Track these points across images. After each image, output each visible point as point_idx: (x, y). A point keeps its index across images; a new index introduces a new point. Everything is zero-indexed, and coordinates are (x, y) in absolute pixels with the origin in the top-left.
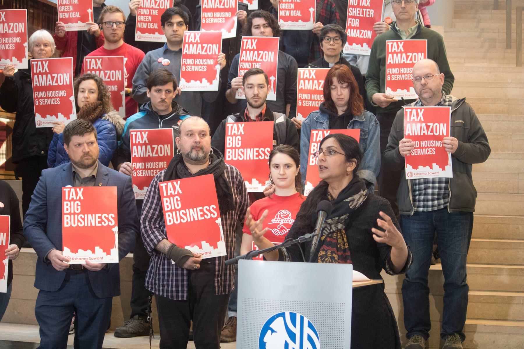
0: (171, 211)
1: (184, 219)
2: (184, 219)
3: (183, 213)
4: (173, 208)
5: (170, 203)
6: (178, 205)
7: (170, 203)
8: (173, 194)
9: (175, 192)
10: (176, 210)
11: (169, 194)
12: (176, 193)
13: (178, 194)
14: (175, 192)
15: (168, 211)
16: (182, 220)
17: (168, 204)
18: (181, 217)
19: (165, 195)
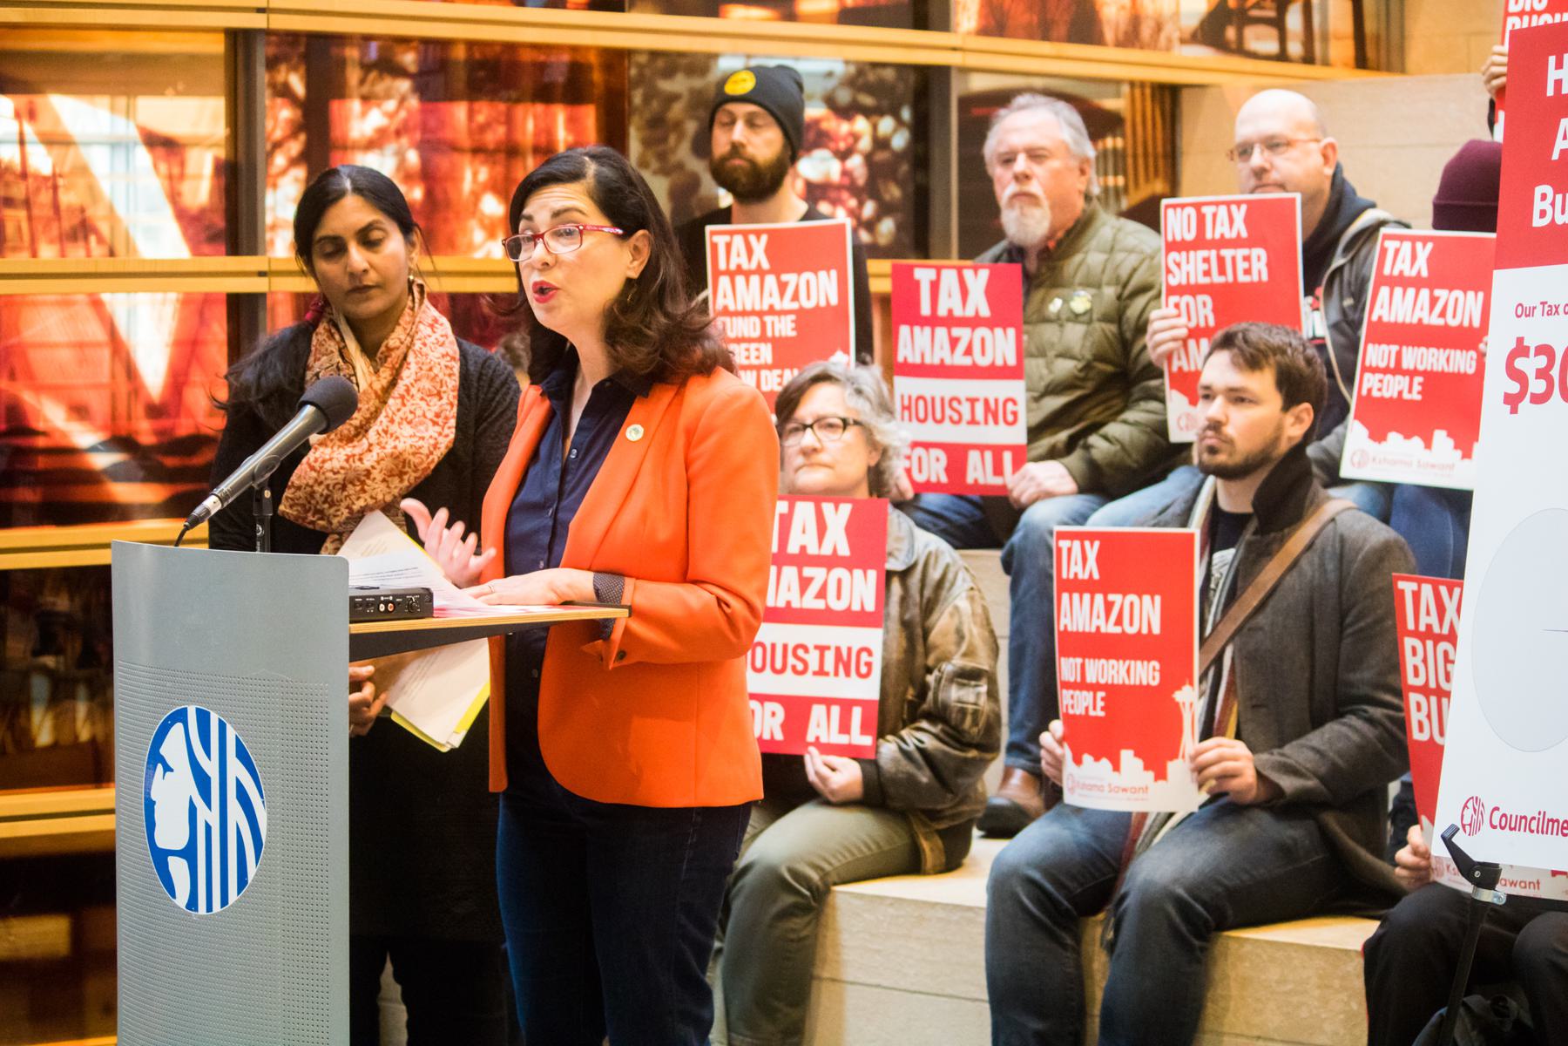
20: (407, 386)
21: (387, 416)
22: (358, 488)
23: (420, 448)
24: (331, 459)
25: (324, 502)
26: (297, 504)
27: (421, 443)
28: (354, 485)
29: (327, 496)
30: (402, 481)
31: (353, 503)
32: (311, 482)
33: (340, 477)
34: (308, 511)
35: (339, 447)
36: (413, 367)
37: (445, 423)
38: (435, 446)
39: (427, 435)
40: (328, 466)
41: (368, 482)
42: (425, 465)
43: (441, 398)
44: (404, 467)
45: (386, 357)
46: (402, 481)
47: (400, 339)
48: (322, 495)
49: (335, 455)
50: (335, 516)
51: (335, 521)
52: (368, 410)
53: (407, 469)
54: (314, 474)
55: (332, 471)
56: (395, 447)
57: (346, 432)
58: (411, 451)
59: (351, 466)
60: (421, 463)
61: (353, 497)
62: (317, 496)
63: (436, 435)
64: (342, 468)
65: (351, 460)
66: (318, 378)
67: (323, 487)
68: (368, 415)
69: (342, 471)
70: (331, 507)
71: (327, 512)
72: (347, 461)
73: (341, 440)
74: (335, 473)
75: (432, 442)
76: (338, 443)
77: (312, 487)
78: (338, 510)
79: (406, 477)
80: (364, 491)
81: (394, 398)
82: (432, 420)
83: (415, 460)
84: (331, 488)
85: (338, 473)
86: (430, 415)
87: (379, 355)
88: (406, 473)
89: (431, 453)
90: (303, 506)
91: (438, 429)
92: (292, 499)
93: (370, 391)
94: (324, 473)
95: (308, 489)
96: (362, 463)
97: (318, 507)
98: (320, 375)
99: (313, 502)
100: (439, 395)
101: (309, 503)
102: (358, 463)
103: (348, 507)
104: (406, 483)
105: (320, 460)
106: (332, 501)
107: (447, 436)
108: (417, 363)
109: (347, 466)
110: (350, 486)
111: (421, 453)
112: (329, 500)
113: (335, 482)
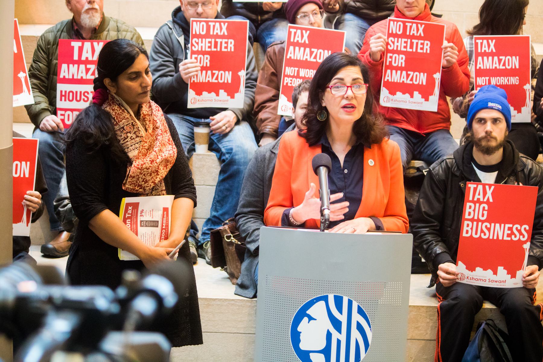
0: (472, 220)
1: (485, 235)
2: (485, 235)
3: (486, 226)
4: (476, 218)
5: (474, 210)
6: (483, 215)
7: (474, 210)
8: (481, 200)
9: (484, 198)
10: (478, 220)
11: (475, 199)
12: (485, 200)
13: (488, 202)
14: (484, 198)
15: (468, 220)
16: (482, 234)
17: (471, 211)
18: (482, 231)
19: (471, 199)
20: (160, 129)
21: (160, 143)
22: (156, 174)
23: (171, 154)
24: (145, 163)
25: (142, 182)
26: (133, 184)
27: (170, 152)
28: (154, 173)
29: (144, 179)
30: (167, 168)
31: (155, 180)
32: (138, 174)
33: (150, 170)
34: (135, 186)
35: (143, 158)
36: (158, 121)
37: (172, 143)
38: (174, 152)
39: (169, 149)
40: (144, 166)
41: (159, 171)
42: (173, 161)
43: (167, 134)
44: (167, 163)
45: (144, 118)
46: (167, 168)
47: (146, 111)
48: (142, 178)
49: (145, 161)
50: (147, 187)
51: (147, 188)
52: (149, 142)
53: (168, 163)
54: (139, 171)
55: (146, 168)
56: (165, 156)
57: (144, 152)
58: (169, 156)
59: (153, 165)
60: (172, 161)
61: (154, 178)
62: (140, 179)
63: (172, 149)
64: (150, 167)
65: (153, 163)
66: (124, 129)
67: (142, 175)
68: (150, 144)
69: (150, 168)
70: (145, 184)
71: (143, 186)
72: (151, 163)
73: (143, 156)
74: (147, 169)
75: (172, 151)
76: (142, 157)
77: (139, 175)
78: (148, 184)
79: (168, 167)
80: (158, 175)
81: (159, 136)
82: (168, 142)
83: (170, 159)
84: (146, 175)
85: (149, 169)
86: (167, 141)
87: (141, 117)
88: (168, 165)
89: (174, 155)
90: (135, 184)
91: (171, 146)
92: (131, 182)
93: (149, 134)
94: (143, 170)
95: (137, 177)
96: (157, 164)
97: (140, 184)
98: (125, 128)
99: (138, 182)
100: (166, 132)
101: (137, 182)
102: (156, 164)
103: (152, 182)
104: (168, 170)
105: (140, 164)
106: (146, 180)
107: (175, 148)
108: (158, 119)
109: (152, 166)
110: (153, 174)
111: (171, 156)
112: (145, 180)
113: (147, 172)
